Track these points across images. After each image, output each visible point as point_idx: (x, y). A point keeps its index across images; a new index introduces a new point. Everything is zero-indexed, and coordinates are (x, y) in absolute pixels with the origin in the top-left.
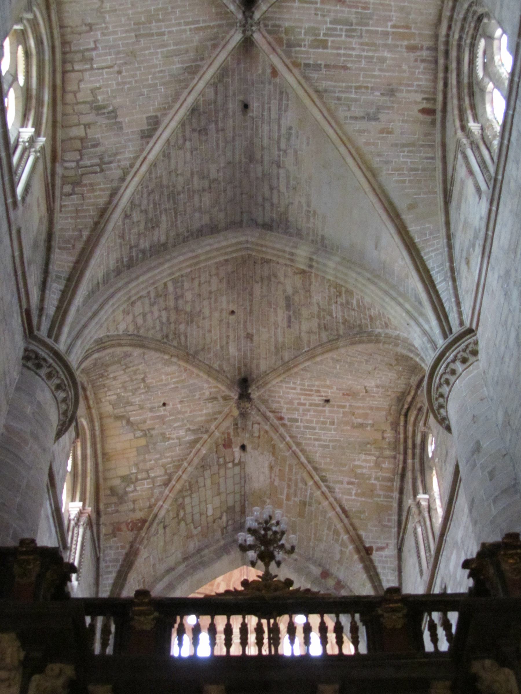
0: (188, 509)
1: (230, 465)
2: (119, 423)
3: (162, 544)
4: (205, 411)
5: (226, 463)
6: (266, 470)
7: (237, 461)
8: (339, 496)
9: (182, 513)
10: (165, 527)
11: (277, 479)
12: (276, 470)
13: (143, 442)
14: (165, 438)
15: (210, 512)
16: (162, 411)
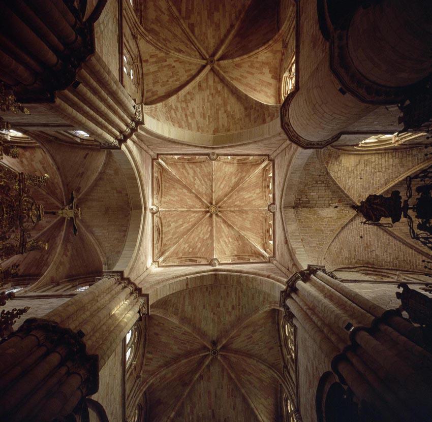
0: (320, 185)
1: (331, 202)
2: (358, 161)
3: (314, 173)
4: (355, 193)
5: (332, 200)
6: (329, 216)
7: (331, 204)
8: (332, 244)
9: (319, 182)
10: (320, 175)
11: (327, 220)
12: (331, 220)
13: (350, 169)
14: (349, 178)
15: (311, 194)
16: (359, 177)
